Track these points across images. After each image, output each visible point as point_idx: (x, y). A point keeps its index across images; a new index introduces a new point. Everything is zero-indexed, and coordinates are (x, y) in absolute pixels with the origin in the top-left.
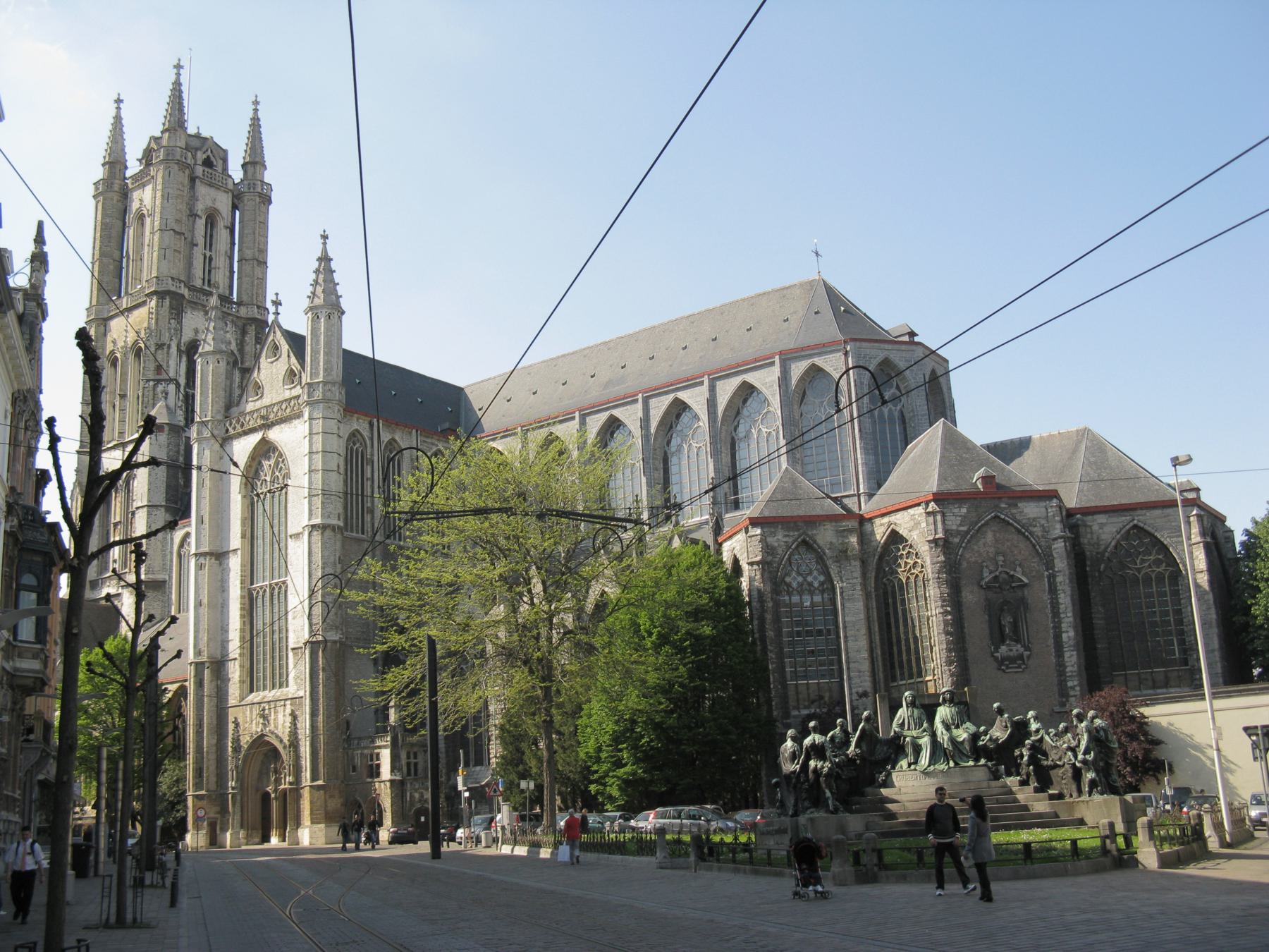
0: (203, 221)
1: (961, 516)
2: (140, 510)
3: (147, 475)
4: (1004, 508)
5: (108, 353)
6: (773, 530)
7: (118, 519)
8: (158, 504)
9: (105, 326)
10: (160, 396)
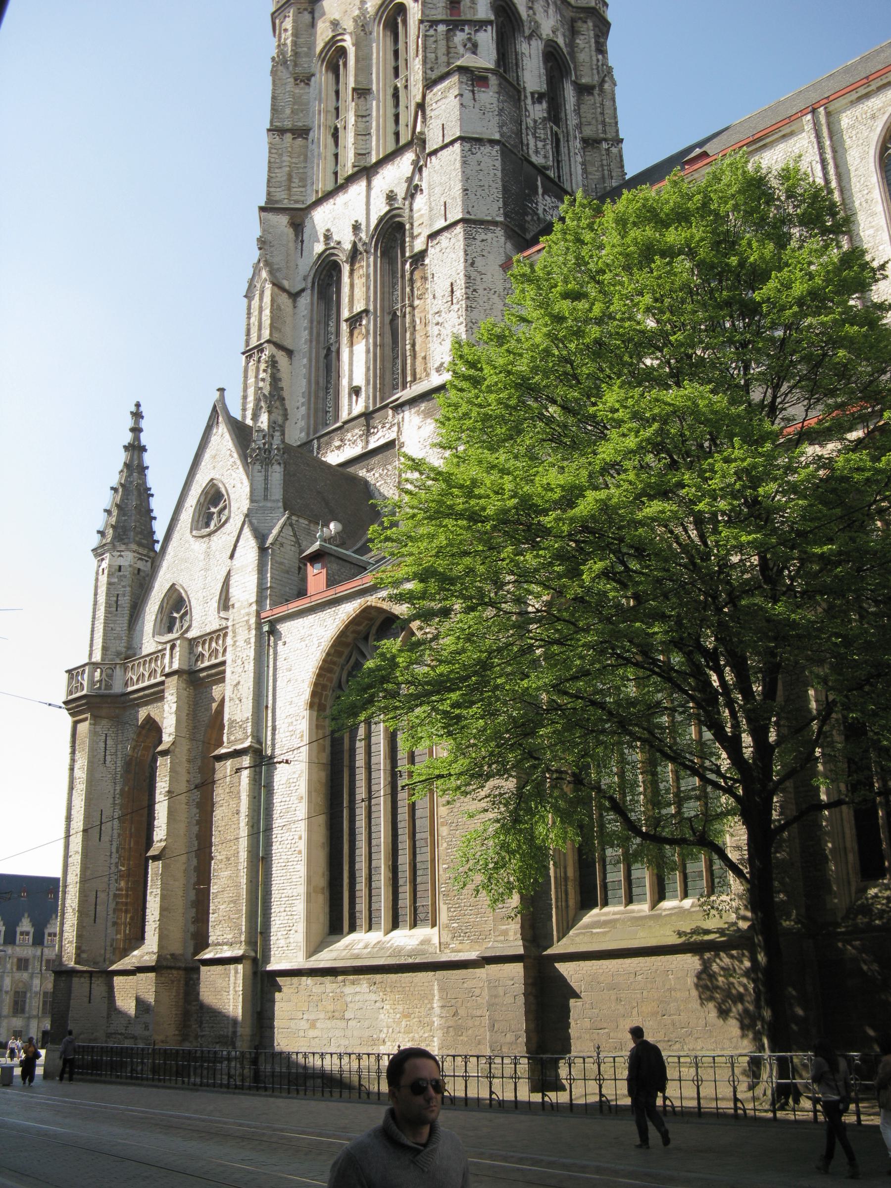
2: (444, 238)
3: (458, 165)
5: (318, 49)
7: (359, 307)
8: (489, 218)
9: (312, 12)
10: (461, 50)
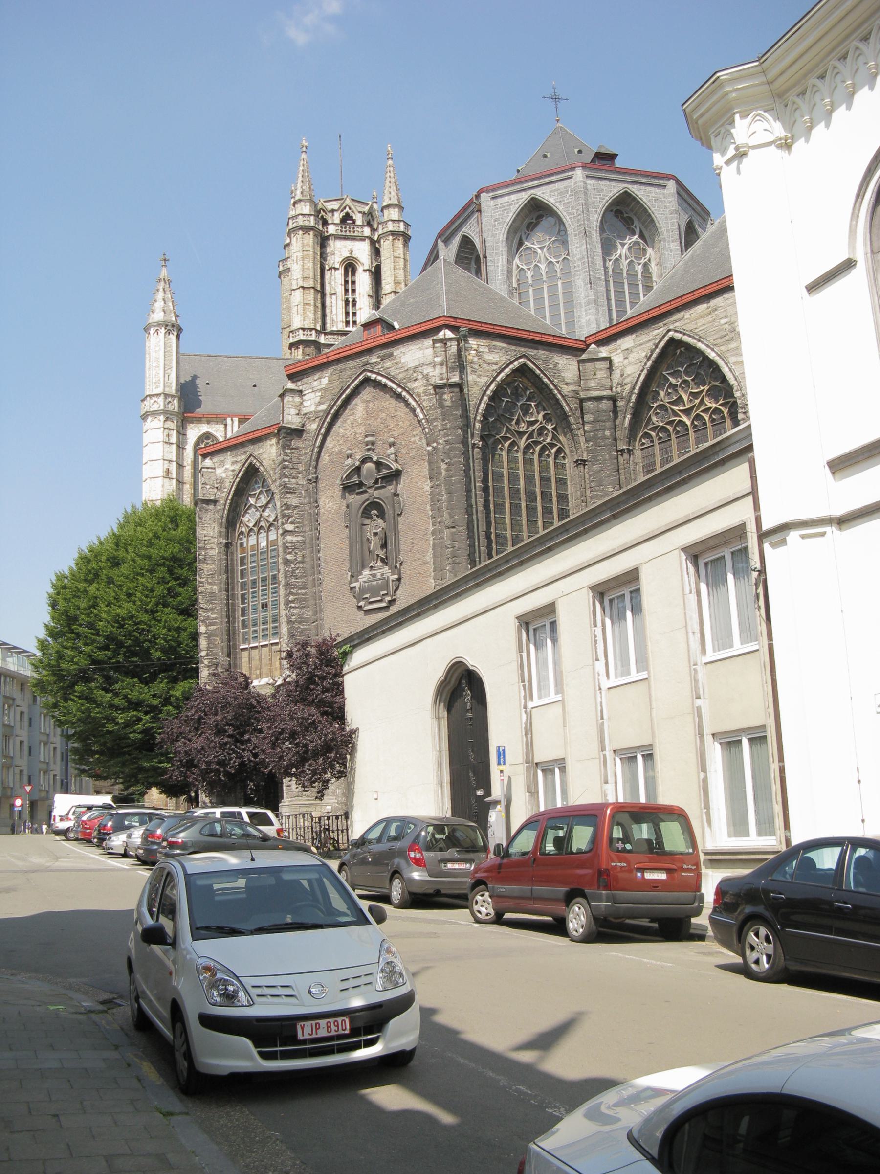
0: (341, 271)
1: (321, 389)
4: (376, 363)
6: (222, 459)
